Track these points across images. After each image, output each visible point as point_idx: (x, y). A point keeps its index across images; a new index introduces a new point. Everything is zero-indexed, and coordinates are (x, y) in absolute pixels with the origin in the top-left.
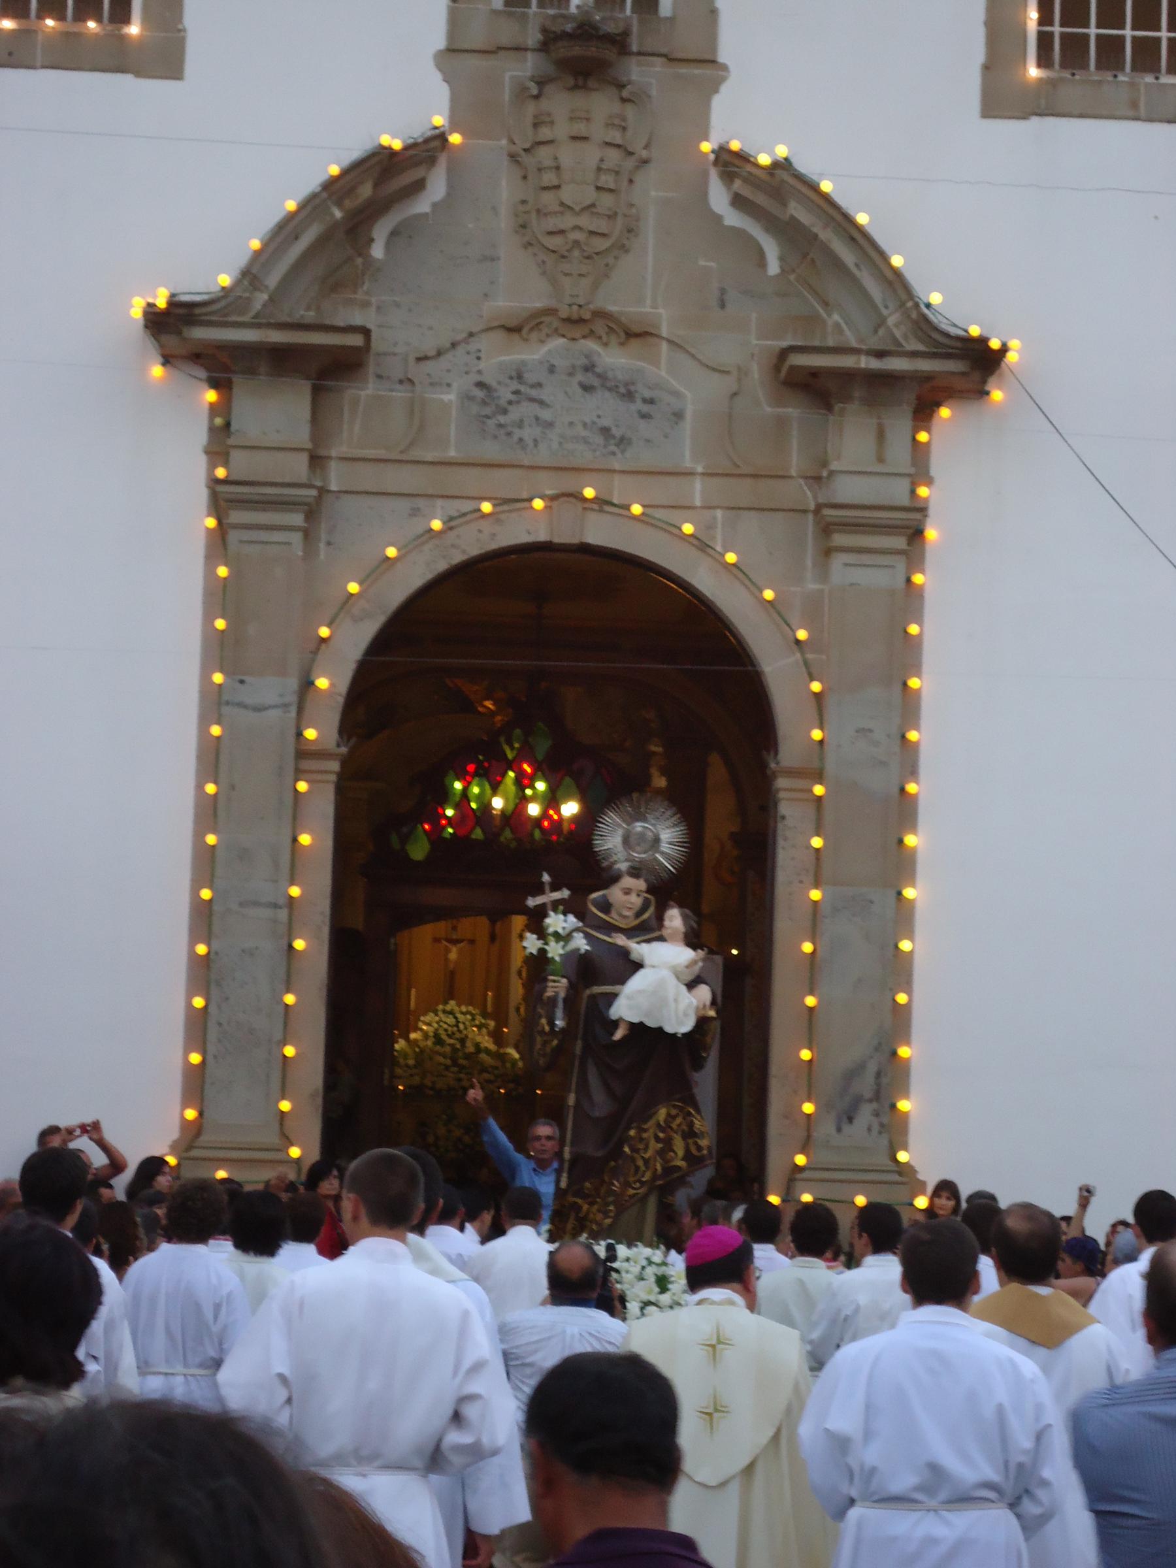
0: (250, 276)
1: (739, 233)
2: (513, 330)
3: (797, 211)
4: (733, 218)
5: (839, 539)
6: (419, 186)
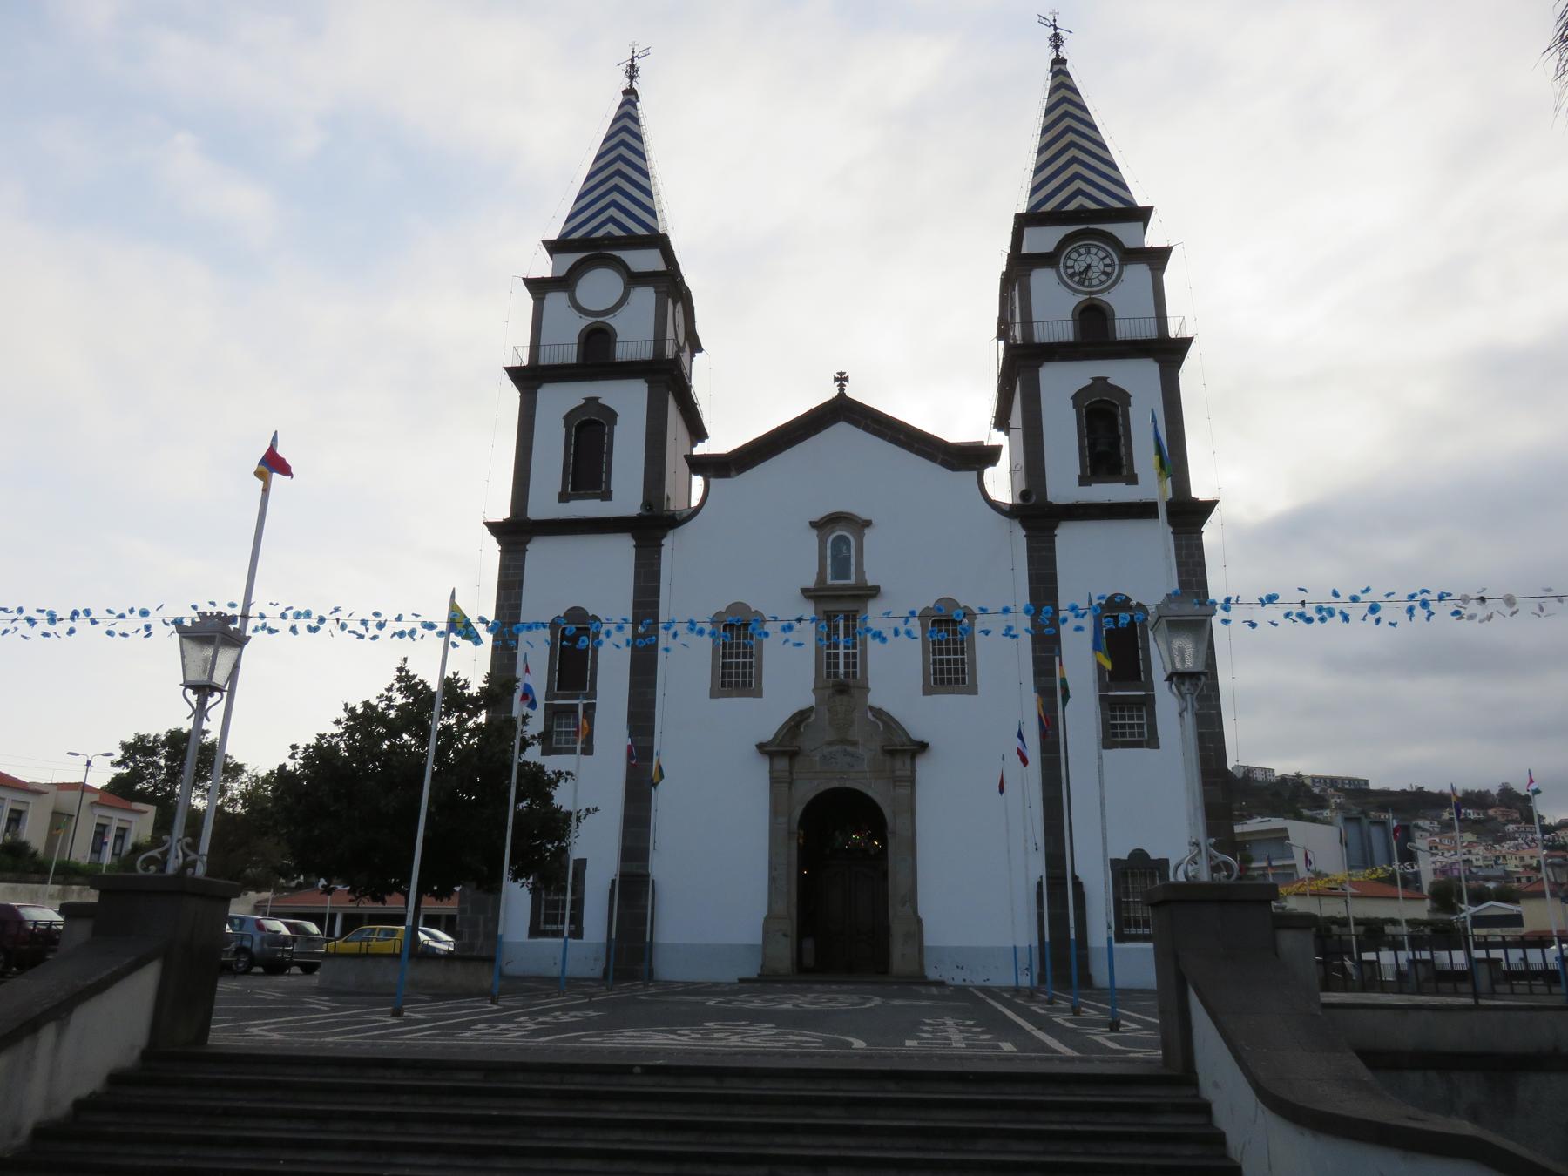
0: (776, 736)
1: (874, 722)
2: (830, 744)
3: (884, 717)
4: (873, 719)
5: (898, 784)
6: (809, 717)
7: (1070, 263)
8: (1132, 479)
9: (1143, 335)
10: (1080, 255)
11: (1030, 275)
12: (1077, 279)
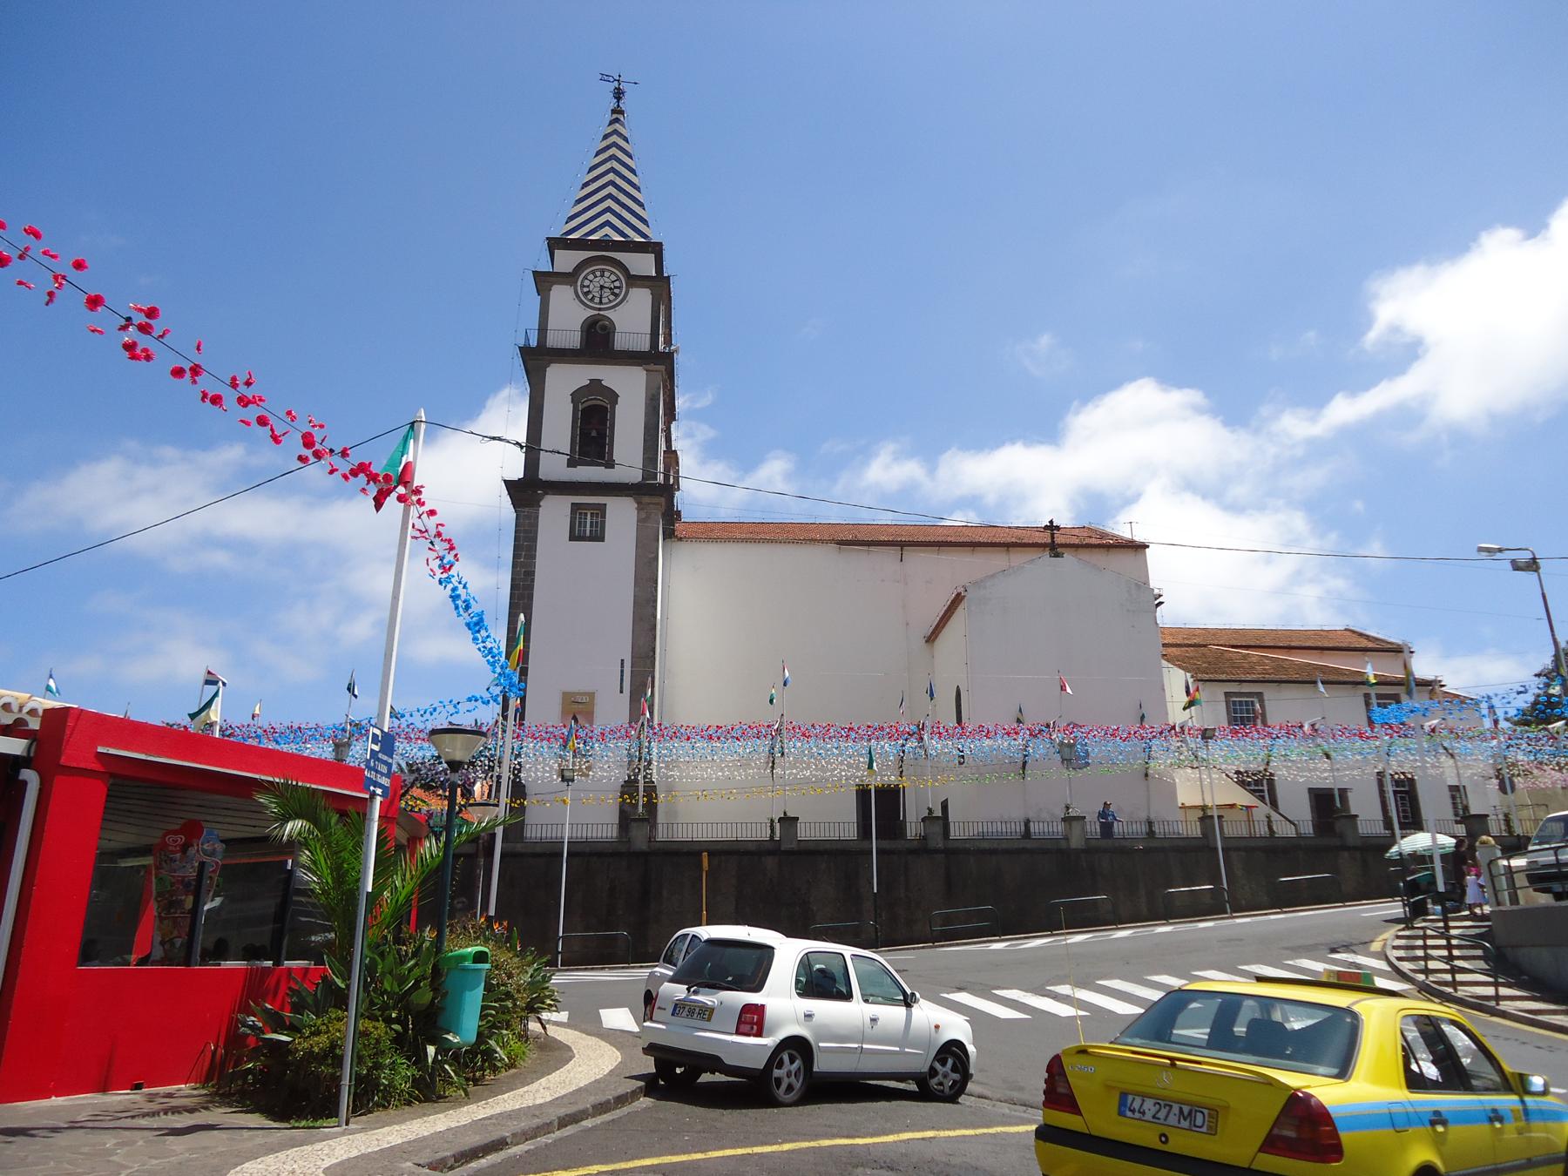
7: (586, 283)
8: (610, 464)
9: (571, 345)
10: (596, 277)
12: (590, 296)
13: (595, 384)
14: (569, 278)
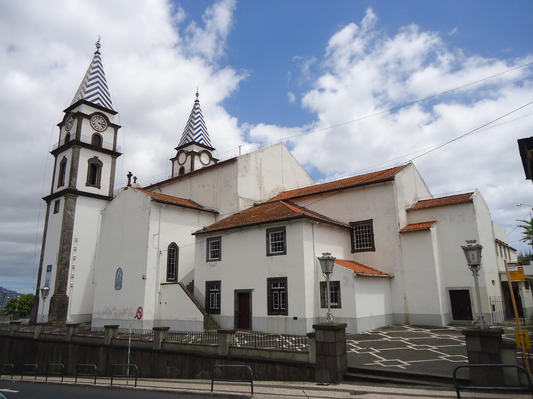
8: (99, 187)
10: (97, 119)
11: (82, 119)
12: (95, 125)
13: (96, 158)
14: (89, 117)
